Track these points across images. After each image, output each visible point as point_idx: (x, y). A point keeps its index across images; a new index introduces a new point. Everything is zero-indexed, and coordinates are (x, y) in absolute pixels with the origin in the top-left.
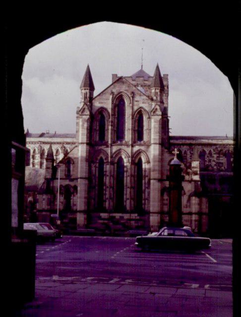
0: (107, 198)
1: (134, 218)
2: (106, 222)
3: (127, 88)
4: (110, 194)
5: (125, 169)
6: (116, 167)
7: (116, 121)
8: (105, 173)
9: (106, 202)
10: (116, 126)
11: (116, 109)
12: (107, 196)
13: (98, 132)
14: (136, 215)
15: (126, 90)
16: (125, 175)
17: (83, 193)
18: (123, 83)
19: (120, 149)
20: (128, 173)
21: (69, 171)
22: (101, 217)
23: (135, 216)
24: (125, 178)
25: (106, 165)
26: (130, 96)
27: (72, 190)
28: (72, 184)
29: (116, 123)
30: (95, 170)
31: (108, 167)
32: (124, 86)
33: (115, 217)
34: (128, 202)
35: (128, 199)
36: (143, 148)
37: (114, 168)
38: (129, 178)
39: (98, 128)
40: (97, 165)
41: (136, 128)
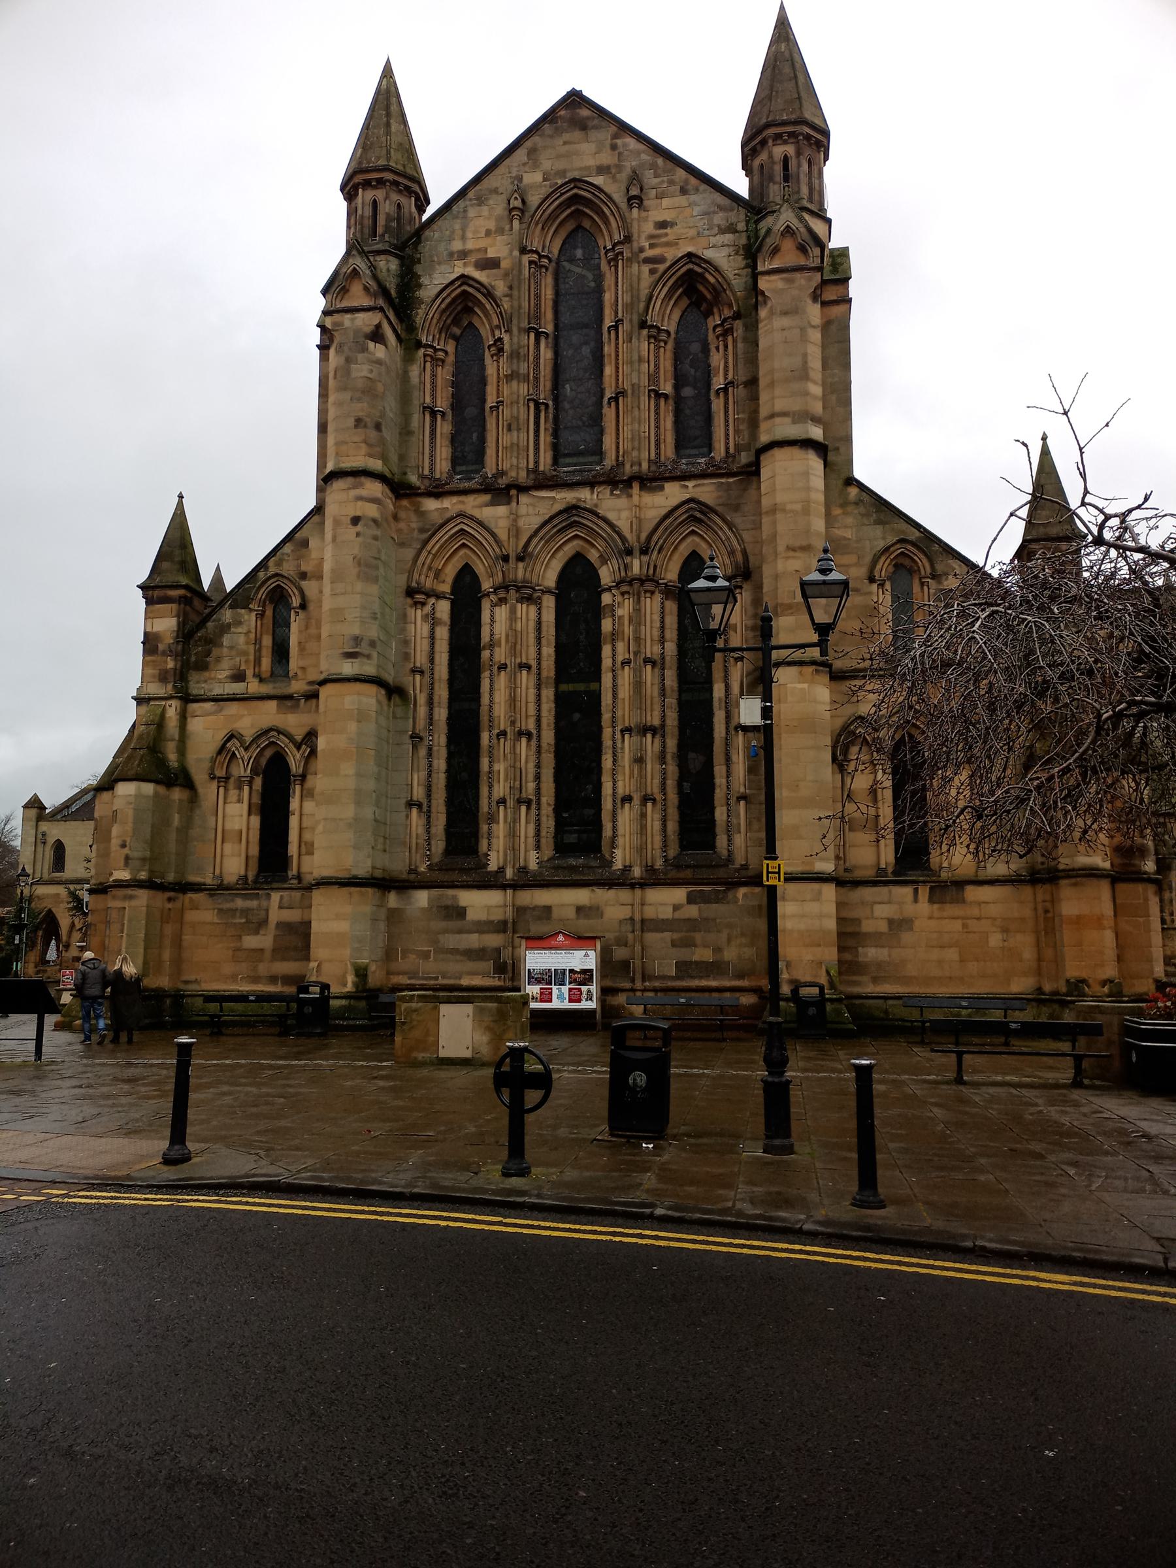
0: (502, 801)
1: (667, 913)
2: (493, 940)
3: (606, 158)
4: (516, 773)
5: (607, 625)
6: (549, 616)
7: (546, 354)
8: (485, 654)
9: (492, 819)
10: (546, 383)
11: (548, 293)
12: (500, 790)
13: (444, 428)
14: (679, 894)
15: (602, 170)
16: (607, 662)
17: (348, 769)
18: (583, 126)
19: (572, 508)
20: (620, 646)
21: (281, 652)
22: (461, 912)
23: (666, 900)
24: (607, 679)
25: (494, 605)
26: (619, 197)
27: (295, 760)
28: (295, 722)
29: (546, 371)
30: (432, 637)
31: (502, 613)
32: (587, 148)
33: (548, 909)
34: (626, 817)
35: (627, 799)
36: (706, 491)
37: (539, 623)
38: (626, 676)
39: (442, 404)
40: (444, 608)
41: (667, 388)
